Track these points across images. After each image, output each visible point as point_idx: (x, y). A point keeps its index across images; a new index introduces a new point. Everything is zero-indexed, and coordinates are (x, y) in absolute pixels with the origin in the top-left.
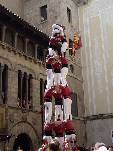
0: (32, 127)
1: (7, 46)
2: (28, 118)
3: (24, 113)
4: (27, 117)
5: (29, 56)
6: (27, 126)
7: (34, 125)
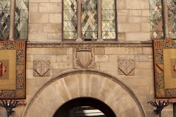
0: (115, 80)
2: (99, 62)
3: (81, 52)
4: (96, 60)
6: (94, 80)
7: (121, 77)
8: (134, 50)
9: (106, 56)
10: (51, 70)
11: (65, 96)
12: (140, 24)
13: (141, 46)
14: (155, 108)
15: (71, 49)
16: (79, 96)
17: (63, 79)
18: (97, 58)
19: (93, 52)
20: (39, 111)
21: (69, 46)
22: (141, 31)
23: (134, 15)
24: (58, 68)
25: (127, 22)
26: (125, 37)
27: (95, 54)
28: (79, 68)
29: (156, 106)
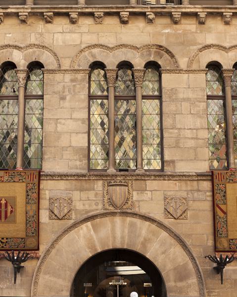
0: (161, 225)
1: (29, 10)
2: (139, 201)
3: (114, 187)
4: (134, 198)
5: (131, 10)
6: (132, 225)
7: (168, 222)
8: (186, 184)
9: (149, 193)
10: (73, 212)
11: (92, 246)
12: (195, 149)
13: (196, 179)
14: (215, 265)
15: (100, 183)
16: (111, 247)
17: (89, 224)
18: (135, 196)
19: (130, 187)
20: (58, 267)
21: (98, 178)
22: (196, 159)
23: (186, 136)
24: (83, 209)
25: (177, 146)
26: (174, 167)
27: (133, 190)
28: (112, 209)
29: (215, 262)
